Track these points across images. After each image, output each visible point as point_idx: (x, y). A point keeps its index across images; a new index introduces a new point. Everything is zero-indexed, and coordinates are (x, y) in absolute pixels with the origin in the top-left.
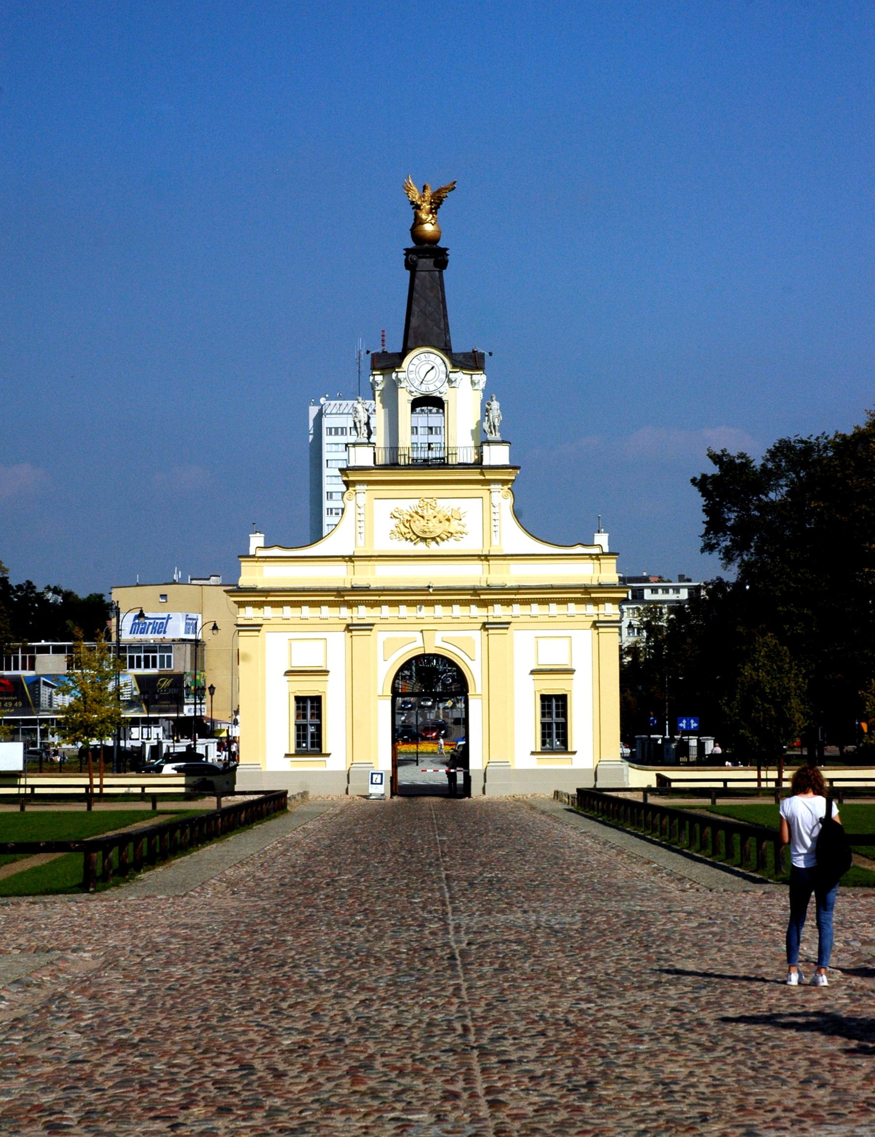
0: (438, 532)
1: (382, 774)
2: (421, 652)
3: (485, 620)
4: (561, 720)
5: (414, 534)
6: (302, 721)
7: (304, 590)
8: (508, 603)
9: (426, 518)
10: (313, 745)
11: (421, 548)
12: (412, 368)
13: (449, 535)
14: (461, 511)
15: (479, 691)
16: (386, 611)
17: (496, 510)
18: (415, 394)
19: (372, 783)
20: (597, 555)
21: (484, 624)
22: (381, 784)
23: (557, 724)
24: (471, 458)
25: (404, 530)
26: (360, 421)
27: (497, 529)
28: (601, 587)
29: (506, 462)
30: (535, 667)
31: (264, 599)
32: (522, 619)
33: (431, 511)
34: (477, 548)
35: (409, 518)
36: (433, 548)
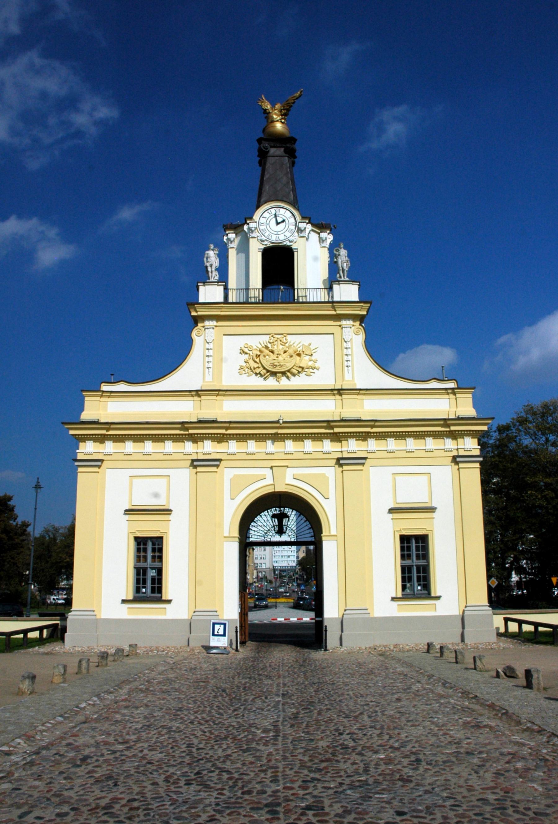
0: (289, 366)
1: (225, 625)
2: (270, 490)
3: (340, 456)
4: (422, 562)
5: (264, 368)
6: (142, 565)
7: (147, 423)
8: (364, 437)
9: (276, 352)
10: (153, 591)
11: (271, 383)
12: (262, 220)
13: (300, 370)
14: (312, 347)
15: (333, 532)
16: (233, 446)
17: (349, 345)
18: (266, 243)
19: (214, 635)
20: (453, 389)
21: (338, 460)
22: (224, 635)
23: (418, 567)
24: (323, 296)
25: (253, 365)
26: (211, 266)
27: (349, 363)
28: (460, 419)
29: (357, 299)
30: (392, 505)
31: (104, 432)
32: (378, 455)
33: (281, 347)
34: (329, 382)
35: (259, 353)
36: (284, 383)
